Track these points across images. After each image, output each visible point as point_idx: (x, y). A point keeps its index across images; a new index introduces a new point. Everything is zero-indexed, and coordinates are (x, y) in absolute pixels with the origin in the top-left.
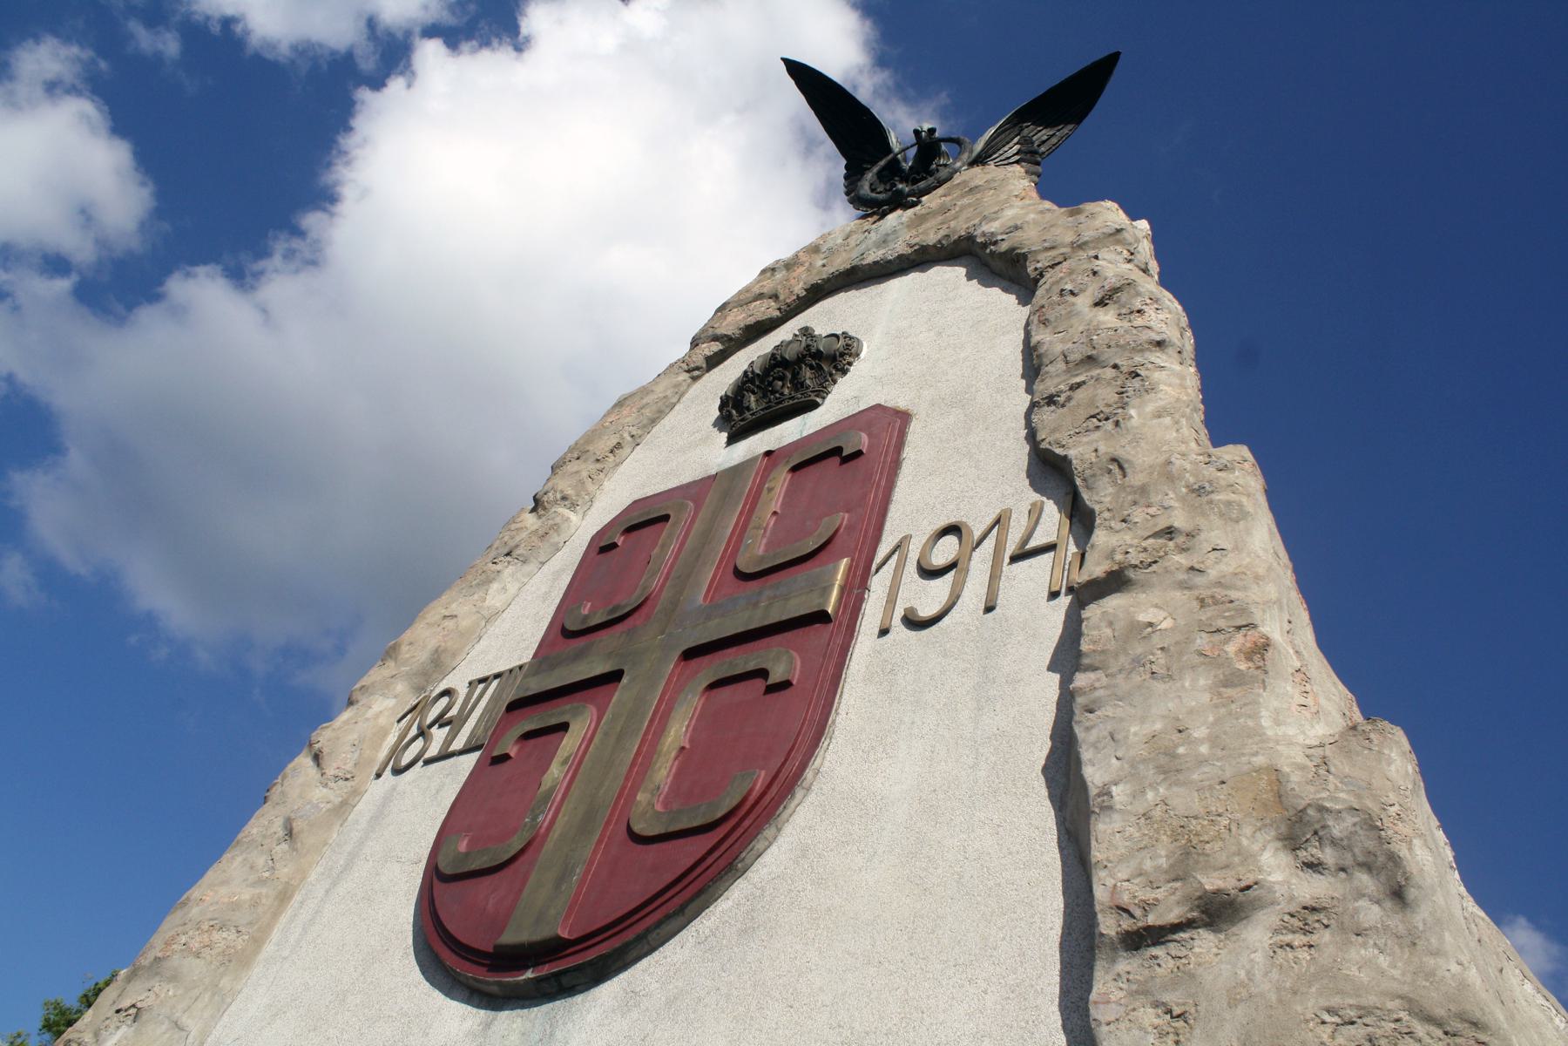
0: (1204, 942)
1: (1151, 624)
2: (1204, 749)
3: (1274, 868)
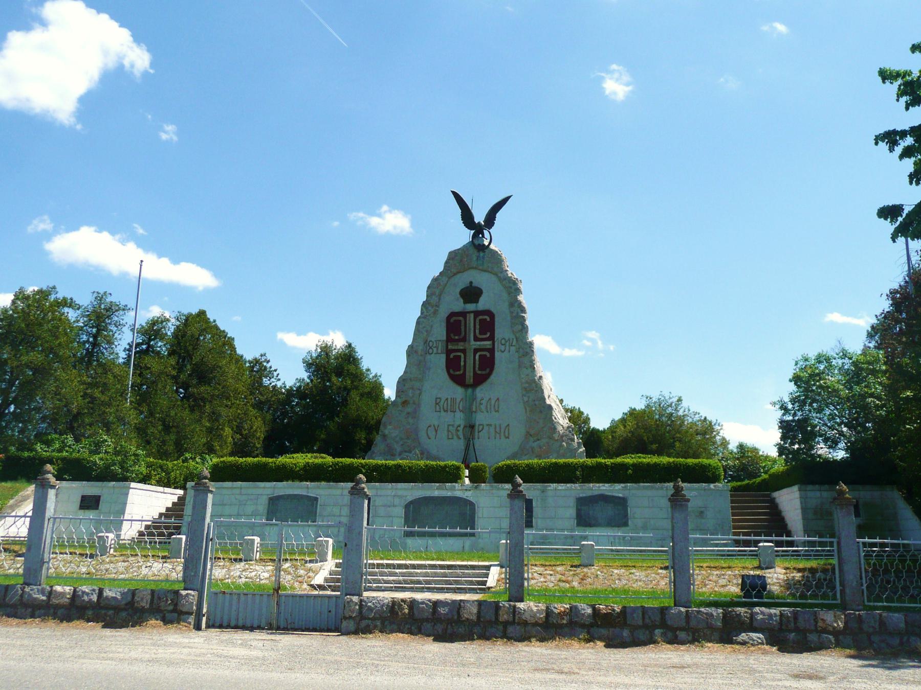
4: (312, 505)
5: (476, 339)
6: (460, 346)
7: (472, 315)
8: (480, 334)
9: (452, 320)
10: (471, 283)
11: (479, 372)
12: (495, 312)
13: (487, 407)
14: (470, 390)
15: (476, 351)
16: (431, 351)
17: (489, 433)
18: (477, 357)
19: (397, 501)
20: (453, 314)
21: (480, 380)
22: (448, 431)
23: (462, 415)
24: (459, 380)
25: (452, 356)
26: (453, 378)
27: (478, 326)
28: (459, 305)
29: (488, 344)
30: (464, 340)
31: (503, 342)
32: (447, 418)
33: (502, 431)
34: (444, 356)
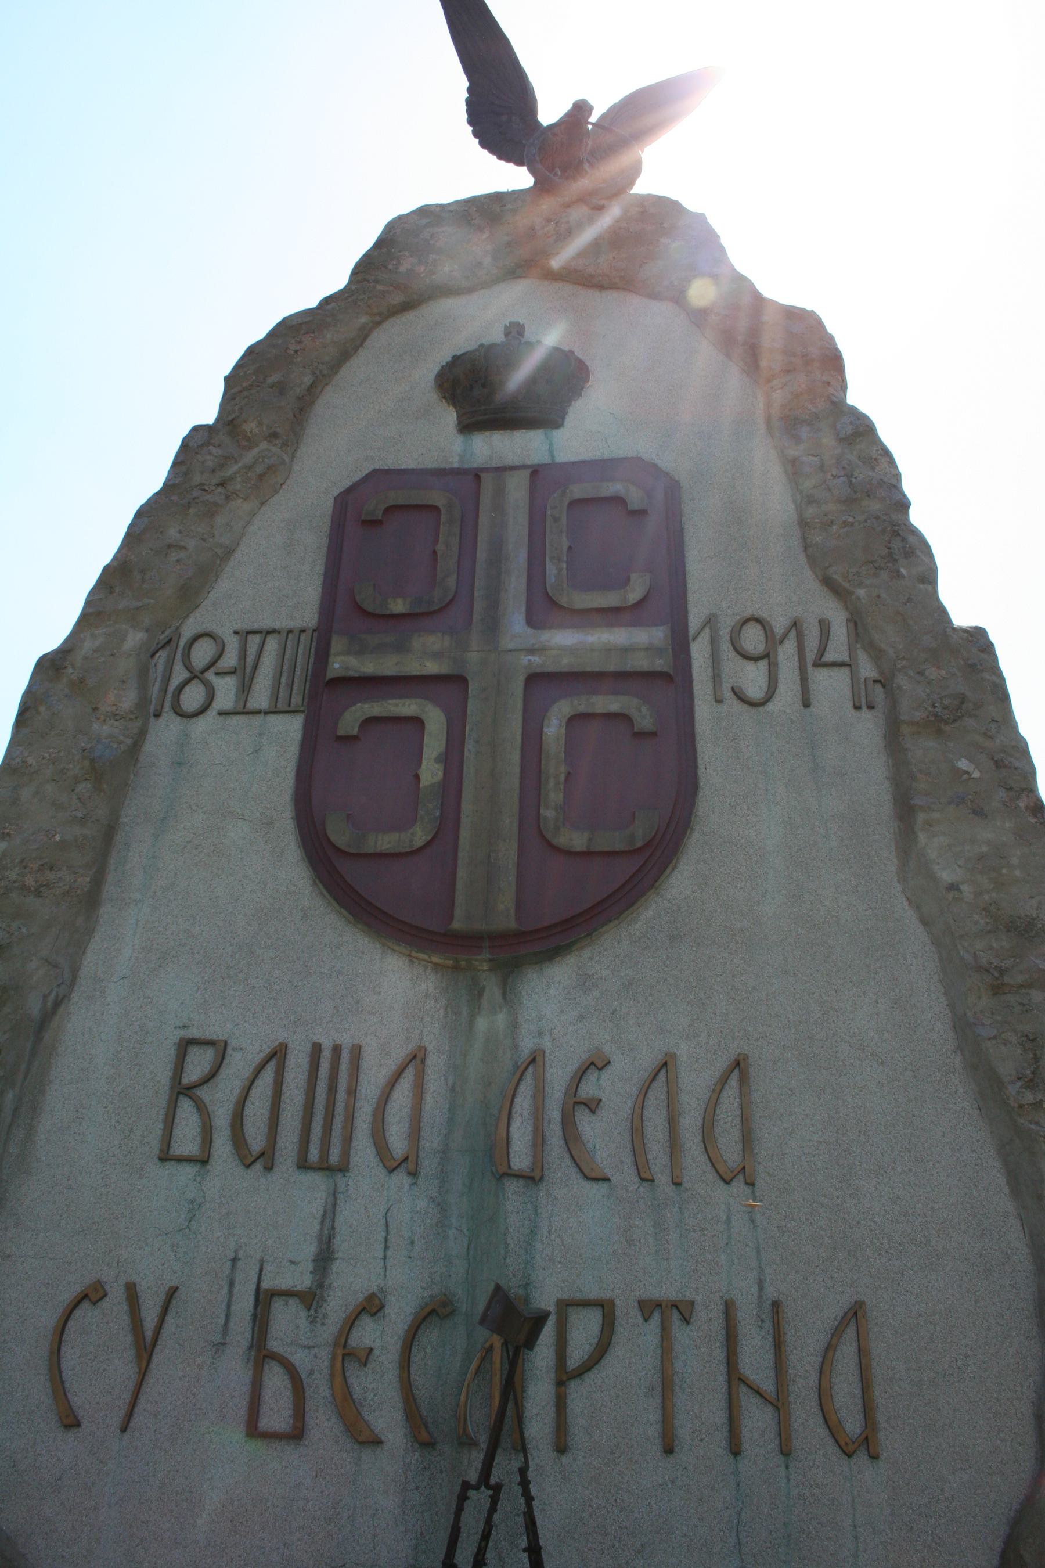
1: (967, 773)
2: (1018, 873)
6: (426, 655)
13: (637, 1130)
16: (193, 697)
17: (666, 1385)
18: (553, 729)
22: (261, 1354)
23: (407, 1203)
26: (350, 878)
31: (753, 639)
33: (803, 1361)
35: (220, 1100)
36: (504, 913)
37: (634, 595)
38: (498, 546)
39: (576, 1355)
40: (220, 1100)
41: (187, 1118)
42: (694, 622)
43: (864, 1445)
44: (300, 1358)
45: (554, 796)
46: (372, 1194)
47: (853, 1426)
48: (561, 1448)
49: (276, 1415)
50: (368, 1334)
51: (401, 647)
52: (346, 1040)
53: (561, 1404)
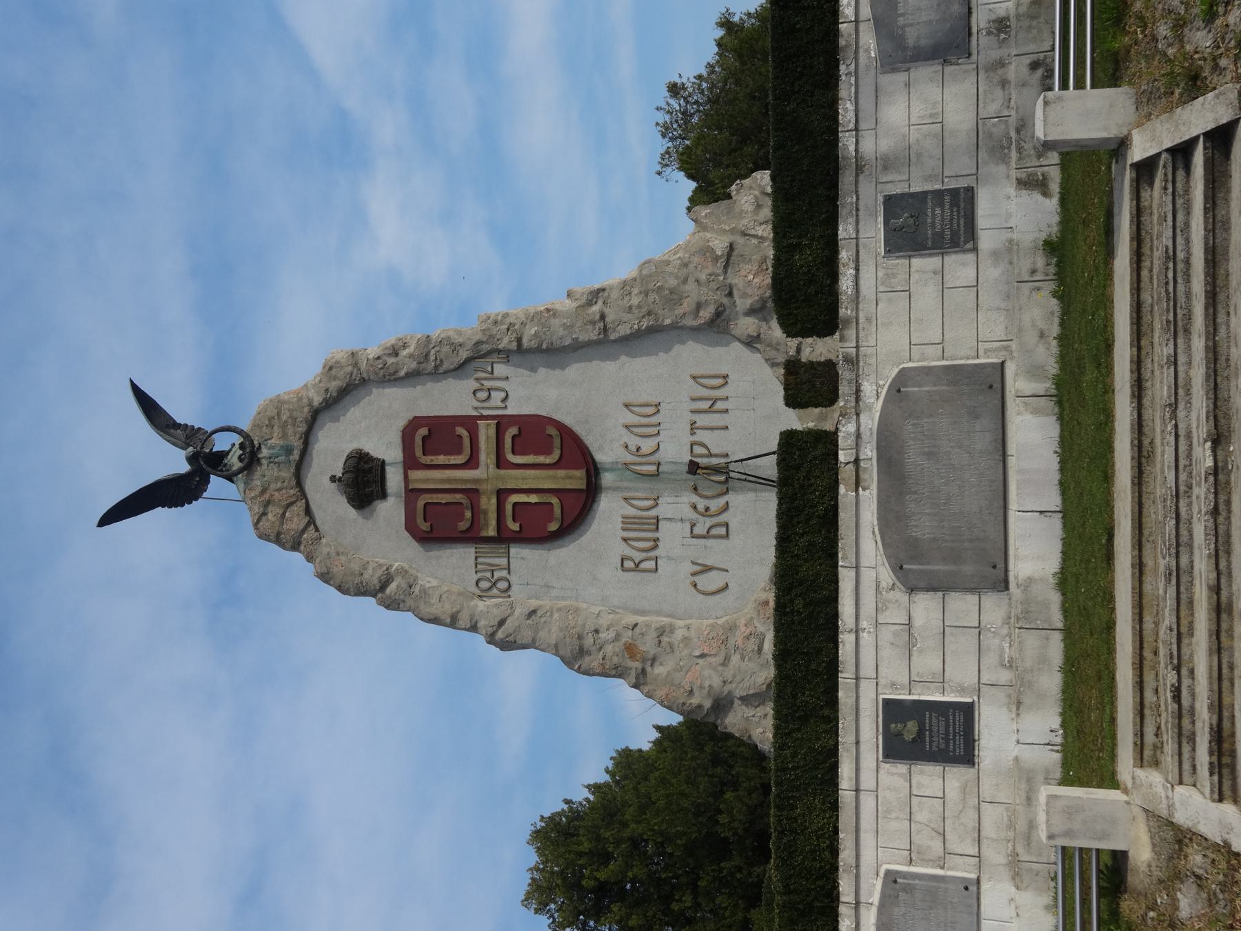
0: (607, 319)
3: (596, 308)
4: (909, 889)
5: (472, 463)
6: (489, 504)
7: (415, 475)
8: (459, 451)
9: (425, 526)
10: (333, 479)
11: (556, 455)
12: (410, 416)
14: (607, 479)
15: (501, 463)
19: (895, 616)
20: (411, 527)
21: (574, 450)
22: (707, 536)
24: (576, 511)
25: (515, 527)
27: (441, 459)
28: (391, 510)
29: (486, 433)
30: (473, 494)
32: (673, 537)
34: (515, 550)
35: (638, 556)
36: (580, 473)
37: (465, 433)
38: (442, 481)
39: (704, 451)
40: (638, 556)
41: (644, 565)
42: (475, 413)
43: (725, 377)
44: (708, 526)
45: (541, 459)
46: (663, 510)
47: (721, 381)
48: (727, 455)
49: (723, 531)
50: (701, 507)
51: (485, 512)
52: (620, 519)
53: (716, 456)
